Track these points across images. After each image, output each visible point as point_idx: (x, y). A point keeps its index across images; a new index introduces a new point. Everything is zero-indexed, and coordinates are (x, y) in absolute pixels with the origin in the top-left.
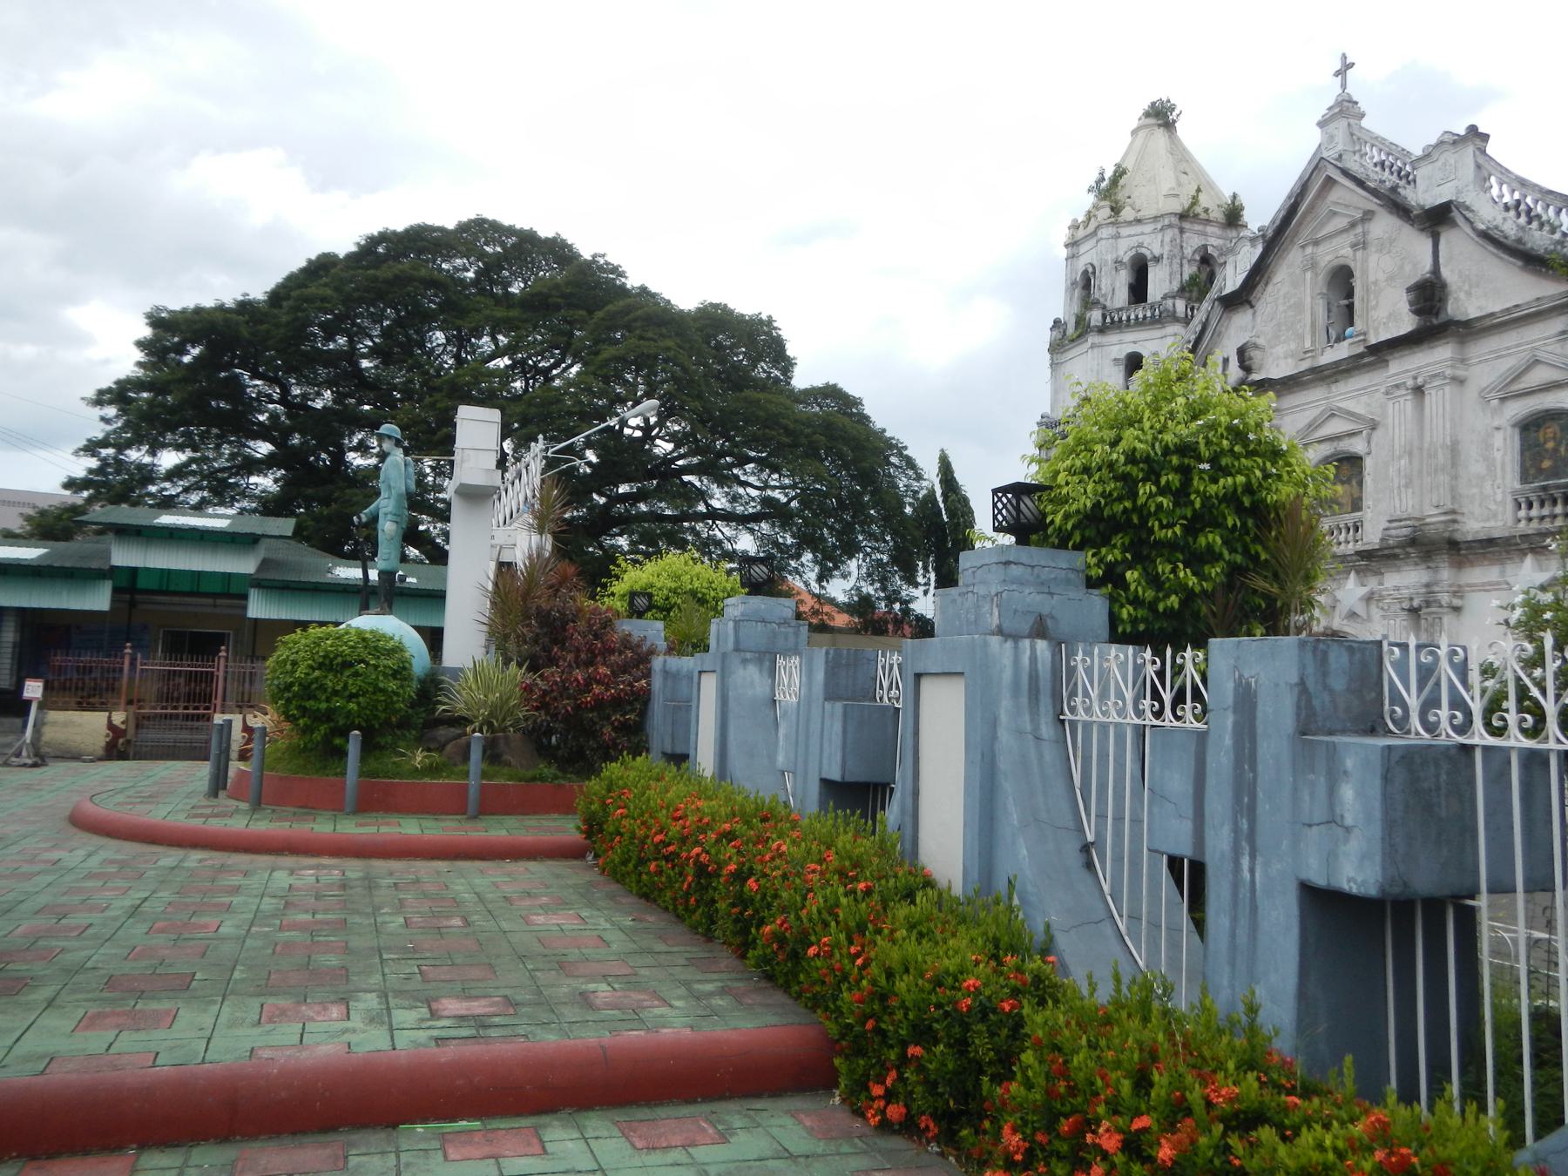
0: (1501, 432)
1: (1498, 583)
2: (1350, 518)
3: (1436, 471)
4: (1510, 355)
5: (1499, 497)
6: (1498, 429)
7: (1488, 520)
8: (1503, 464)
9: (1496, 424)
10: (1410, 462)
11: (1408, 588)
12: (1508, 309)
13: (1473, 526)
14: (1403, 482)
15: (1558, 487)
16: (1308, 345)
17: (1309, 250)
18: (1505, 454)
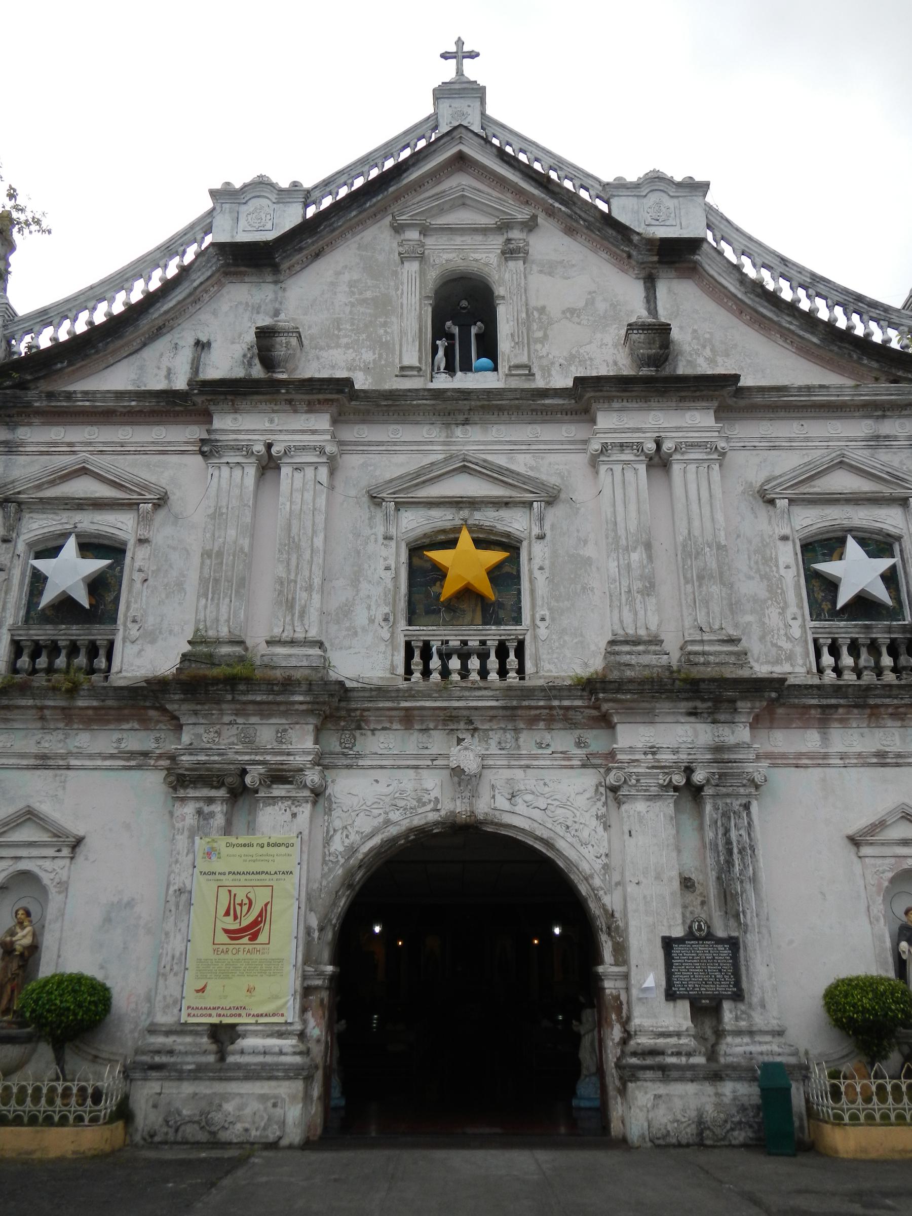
0: (790, 543)
1: (825, 756)
2: (493, 634)
3: (701, 578)
4: (791, 448)
5: (796, 632)
6: (785, 538)
7: (778, 661)
8: (797, 586)
9: (786, 531)
10: (650, 558)
11: (675, 751)
12: (809, 389)
13: (761, 670)
14: (637, 585)
15: (890, 630)
16: (411, 358)
17: (413, 235)
18: (798, 575)
